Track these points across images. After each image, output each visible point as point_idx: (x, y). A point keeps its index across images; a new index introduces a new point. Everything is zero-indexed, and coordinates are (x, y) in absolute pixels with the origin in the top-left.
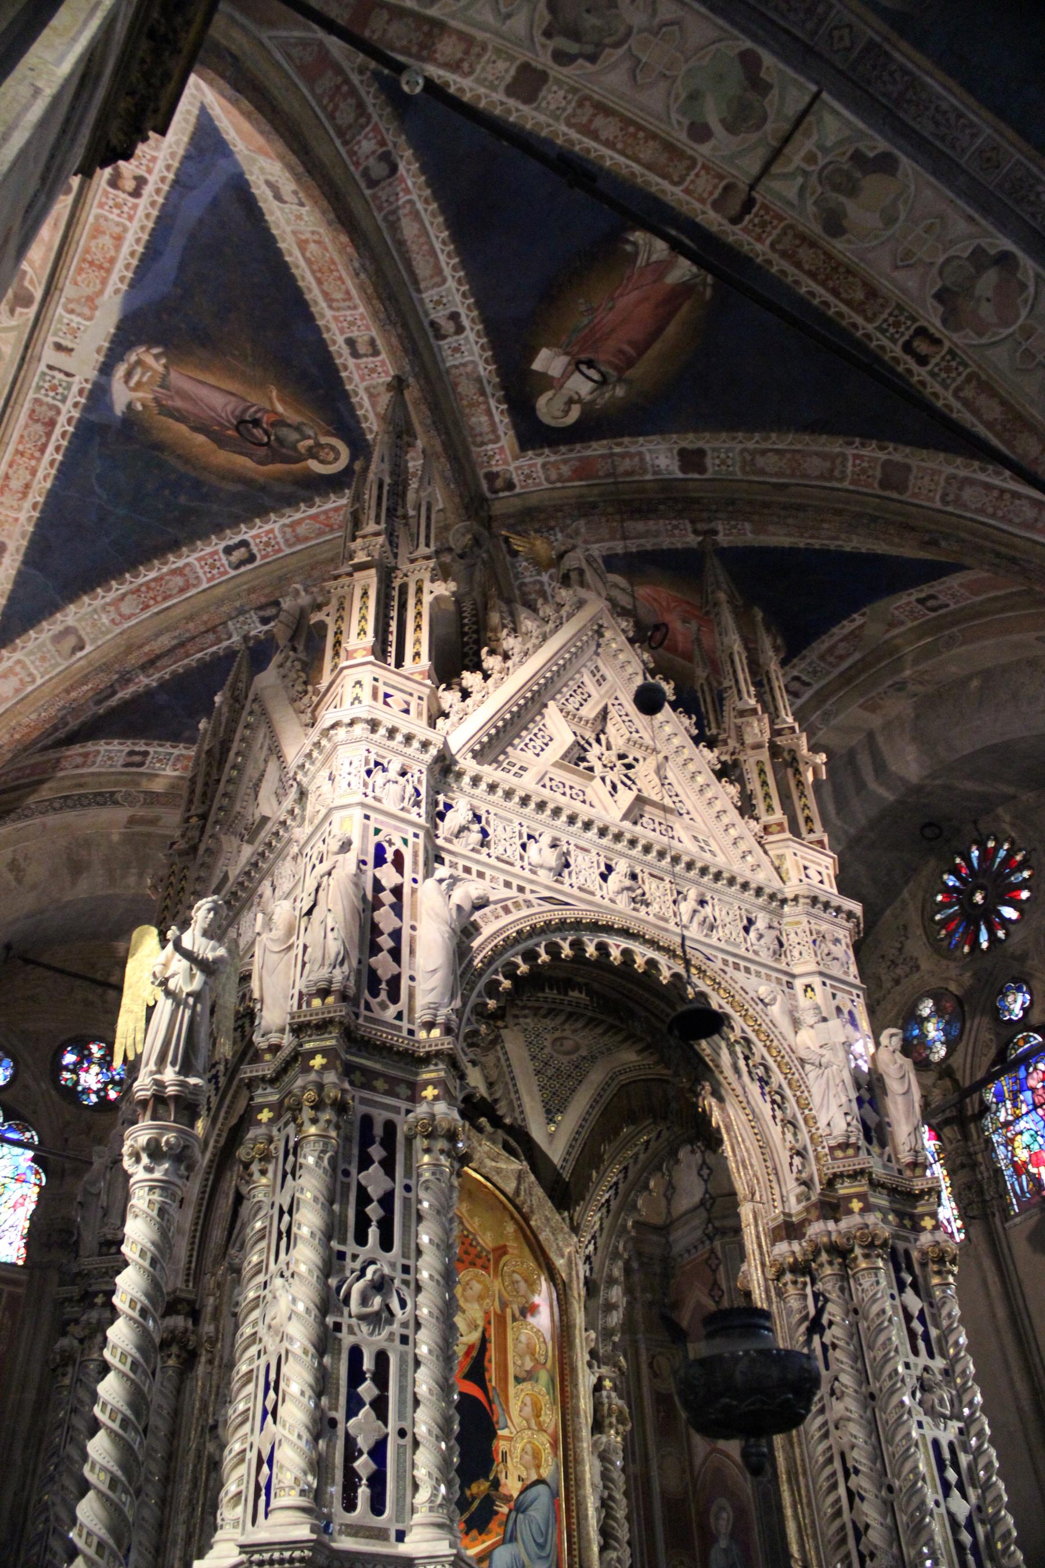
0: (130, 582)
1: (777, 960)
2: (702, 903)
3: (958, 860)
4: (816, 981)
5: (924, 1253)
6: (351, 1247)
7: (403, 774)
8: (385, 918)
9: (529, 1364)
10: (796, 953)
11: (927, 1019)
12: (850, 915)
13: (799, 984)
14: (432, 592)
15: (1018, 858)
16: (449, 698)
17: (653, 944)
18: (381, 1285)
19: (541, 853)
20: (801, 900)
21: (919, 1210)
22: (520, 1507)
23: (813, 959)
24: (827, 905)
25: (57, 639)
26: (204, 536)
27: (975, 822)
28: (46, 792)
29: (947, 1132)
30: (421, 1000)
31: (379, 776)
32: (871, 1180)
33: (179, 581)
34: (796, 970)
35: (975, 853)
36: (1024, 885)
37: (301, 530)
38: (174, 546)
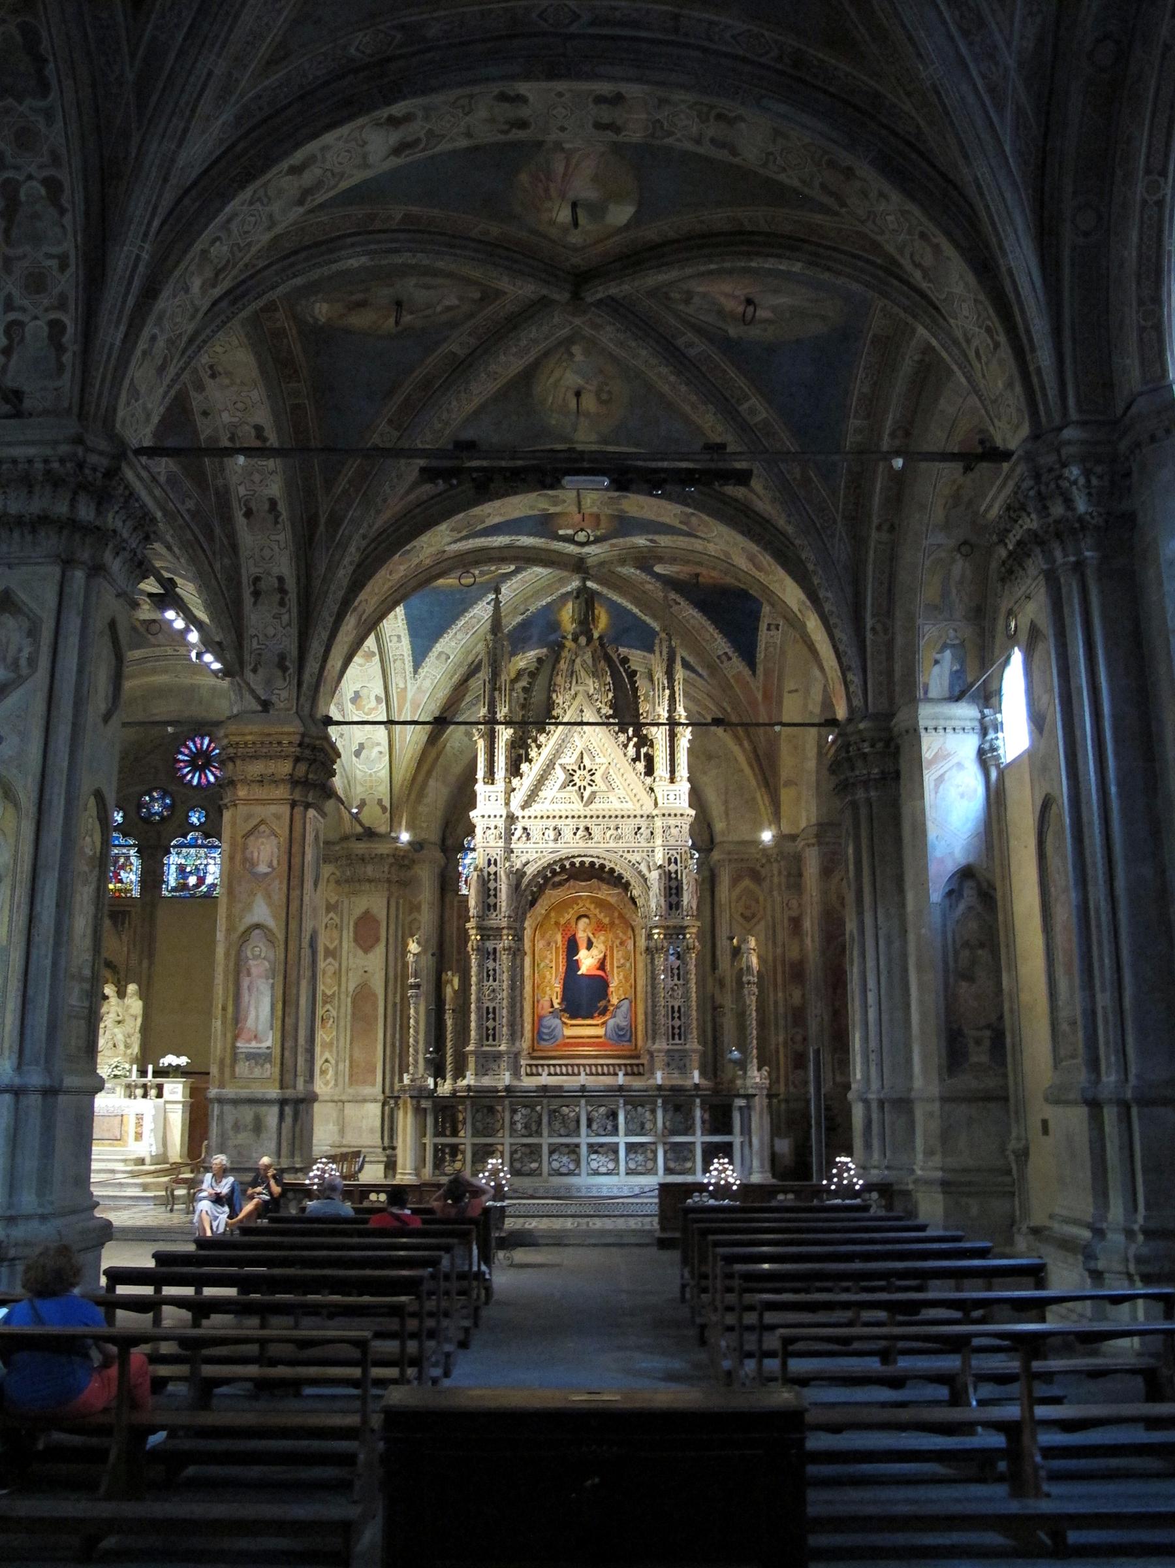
0: (455, 628)
2: (617, 829)
6: (485, 983)
7: (496, 828)
8: (492, 885)
9: (622, 961)
13: (656, 850)
14: (505, 734)
16: (515, 782)
17: (592, 856)
18: (494, 991)
19: (551, 834)
22: (618, 1007)
25: (438, 658)
26: (476, 603)
28: (468, 699)
30: (503, 909)
31: (489, 832)
33: (475, 620)
37: (515, 586)
38: (465, 610)
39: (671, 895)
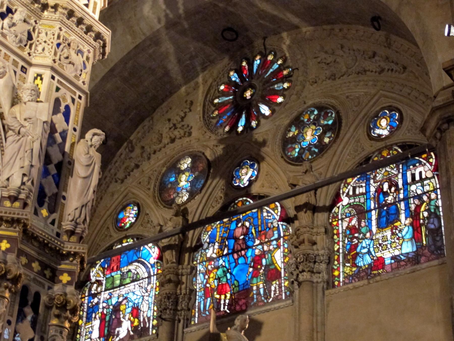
1: (20, 47)
3: (244, 64)
4: (47, 74)
5: (52, 299)
10: (40, 48)
11: (183, 172)
12: (98, 36)
13: (32, 72)
15: (285, 72)
20: (60, 10)
21: (63, 266)
23: (52, 57)
24: (80, 22)
27: (264, 38)
29: (168, 255)
32: (25, 231)
34: (34, 61)
35: (257, 62)
36: (282, 93)
39: (46, 173)
